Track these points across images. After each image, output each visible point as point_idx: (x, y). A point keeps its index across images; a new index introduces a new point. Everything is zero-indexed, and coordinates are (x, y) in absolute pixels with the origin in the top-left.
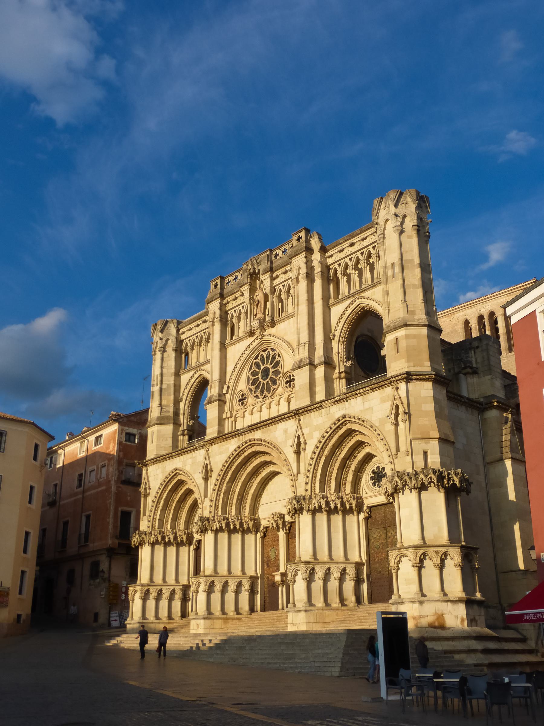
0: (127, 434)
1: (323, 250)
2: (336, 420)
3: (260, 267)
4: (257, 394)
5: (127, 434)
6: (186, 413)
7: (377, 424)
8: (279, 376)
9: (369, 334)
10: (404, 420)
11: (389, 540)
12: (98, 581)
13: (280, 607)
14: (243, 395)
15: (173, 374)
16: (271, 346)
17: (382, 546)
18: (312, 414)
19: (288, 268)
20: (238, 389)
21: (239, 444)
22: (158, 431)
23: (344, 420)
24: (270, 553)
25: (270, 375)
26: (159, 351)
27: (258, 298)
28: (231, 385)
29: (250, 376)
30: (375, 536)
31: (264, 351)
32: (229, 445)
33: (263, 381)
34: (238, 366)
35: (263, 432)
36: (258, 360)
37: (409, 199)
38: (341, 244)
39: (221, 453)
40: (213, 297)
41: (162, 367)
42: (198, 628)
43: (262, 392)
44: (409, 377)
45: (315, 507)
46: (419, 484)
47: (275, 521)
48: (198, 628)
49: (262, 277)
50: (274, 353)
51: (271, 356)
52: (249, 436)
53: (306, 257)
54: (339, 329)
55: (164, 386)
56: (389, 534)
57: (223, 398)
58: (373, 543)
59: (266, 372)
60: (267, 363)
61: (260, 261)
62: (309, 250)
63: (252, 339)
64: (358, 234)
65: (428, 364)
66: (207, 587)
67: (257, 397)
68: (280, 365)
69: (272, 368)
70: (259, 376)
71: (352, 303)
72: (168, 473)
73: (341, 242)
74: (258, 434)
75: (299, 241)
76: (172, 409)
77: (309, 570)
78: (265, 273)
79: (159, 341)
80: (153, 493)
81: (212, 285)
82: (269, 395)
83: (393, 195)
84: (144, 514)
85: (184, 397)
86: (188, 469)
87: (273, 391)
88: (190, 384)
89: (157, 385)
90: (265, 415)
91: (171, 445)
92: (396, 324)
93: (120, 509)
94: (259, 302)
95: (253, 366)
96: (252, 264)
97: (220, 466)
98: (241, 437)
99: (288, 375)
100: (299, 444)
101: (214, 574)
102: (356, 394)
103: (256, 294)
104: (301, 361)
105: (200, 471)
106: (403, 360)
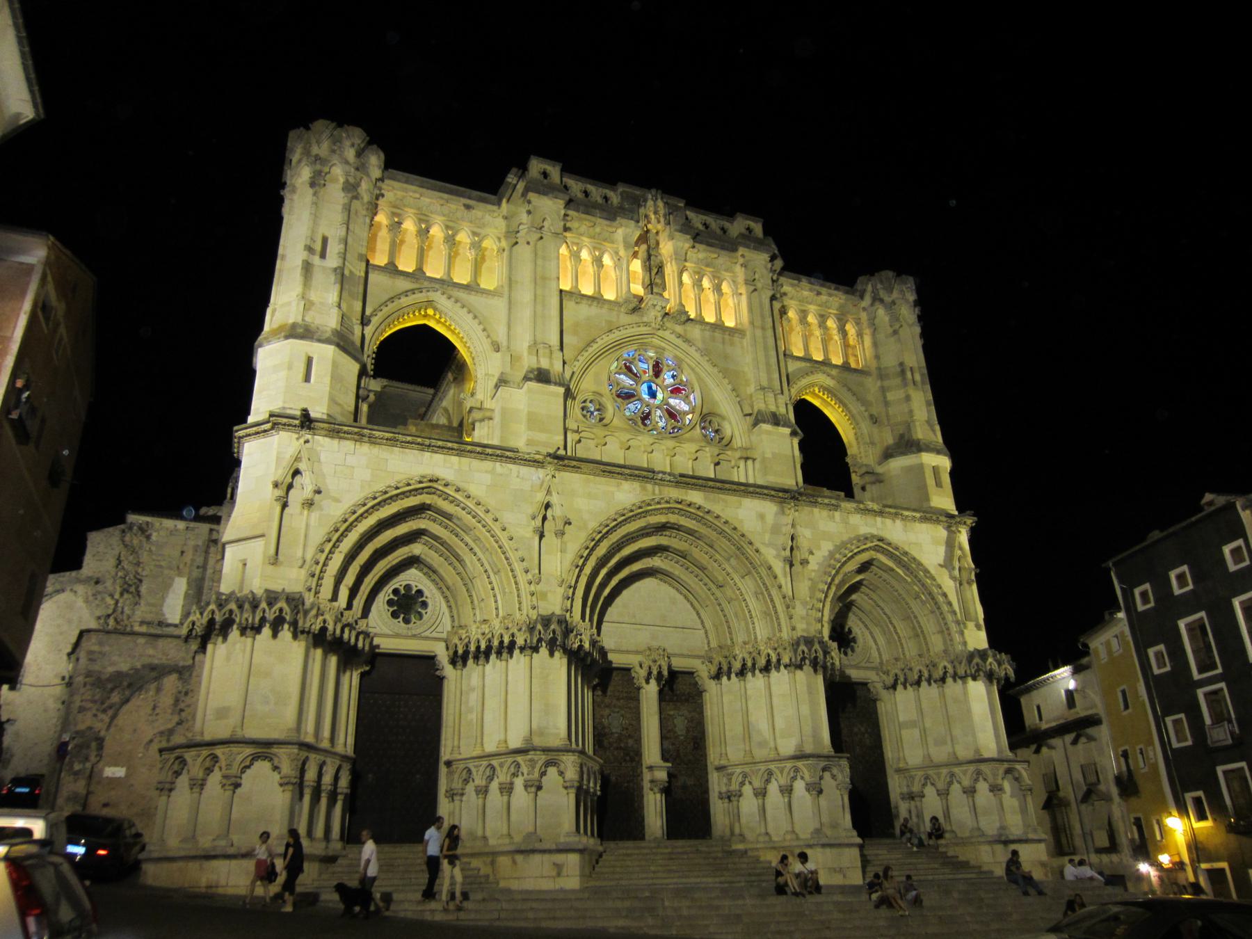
7: (933, 572)
18: (816, 510)
21: (647, 498)
22: (335, 365)
24: (605, 721)
32: (613, 489)
35: (706, 499)
42: (559, 875)
52: (674, 493)
56: (856, 730)
63: (625, 319)
72: (398, 478)
74: (696, 497)
85: (375, 321)
86: (476, 490)
89: (323, 255)
97: (593, 525)
98: (649, 487)
102: (896, 514)
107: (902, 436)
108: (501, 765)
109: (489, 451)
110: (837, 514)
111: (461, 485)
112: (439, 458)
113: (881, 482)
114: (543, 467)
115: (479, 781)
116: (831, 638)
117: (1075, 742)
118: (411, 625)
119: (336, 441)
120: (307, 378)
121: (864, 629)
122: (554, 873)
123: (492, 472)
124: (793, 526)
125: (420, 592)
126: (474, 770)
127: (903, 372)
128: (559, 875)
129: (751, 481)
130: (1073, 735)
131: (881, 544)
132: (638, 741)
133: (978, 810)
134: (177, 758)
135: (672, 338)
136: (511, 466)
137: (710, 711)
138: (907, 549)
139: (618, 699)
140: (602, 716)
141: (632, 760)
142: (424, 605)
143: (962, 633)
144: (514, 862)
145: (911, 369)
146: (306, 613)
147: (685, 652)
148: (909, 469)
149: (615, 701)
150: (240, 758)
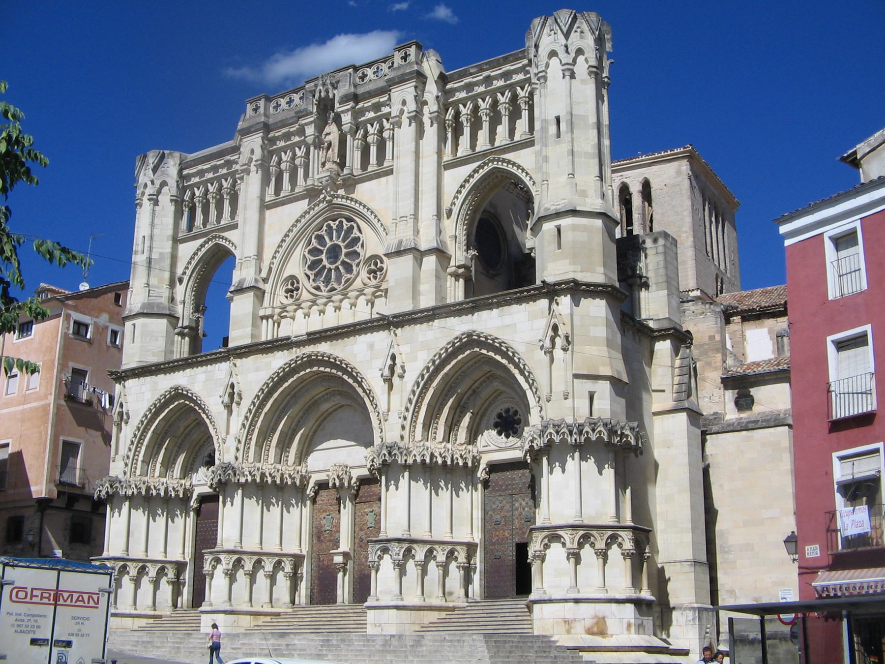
0: (76, 322)
1: (443, 79)
2: (457, 338)
3: (335, 92)
4: (318, 283)
5: (76, 322)
6: (187, 301)
8: (357, 261)
9: (492, 211)
10: (565, 350)
11: (516, 513)
12: (20, 546)
13: (339, 599)
14: (292, 284)
15: (171, 238)
17: (505, 521)
18: (418, 327)
19: (384, 99)
20: (287, 274)
23: (471, 340)
25: (343, 257)
26: (149, 200)
27: (328, 138)
28: (274, 267)
29: (307, 256)
30: (494, 506)
31: (334, 220)
33: (328, 266)
34: (288, 240)
36: (323, 232)
37: (585, 27)
38: (471, 74)
39: (257, 370)
41: (152, 225)
43: (327, 281)
44: (578, 290)
45: (415, 461)
46: (583, 439)
47: (338, 477)
49: (338, 108)
50: (349, 224)
51: (345, 227)
53: (416, 87)
54: (459, 203)
55: (155, 256)
56: (517, 505)
57: (261, 285)
58: (491, 516)
59: (334, 253)
61: (338, 82)
62: (421, 77)
64: (498, 64)
65: (601, 270)
66: (230, 567)
67: (318, 288)
68: (360, 244)
69: (346, 247)
71: (480, 167)
72: (162, 392)
73: (472, 71)
74: (323, 348)
75: (405, 61)
76: (165, 292)
77: (403, 550)
78: (345, 99)
79: (149, 184)
80: (135, 420)
81: (249, 108)
82: (339, 288)
83: (564, 16)
84: (117, 453)
85: (186, 278)
87: (346, 282)
88: (197, 258)
90: (331, 319)
91: (163, 348)
92: (558, 207)
93: (62, 438)
94: (330, 145)
95: (313, 240)
96: (324, 85)
97: (256, 391)
100: (392, 368)
101: (239, 549)
103: (327, 130)
104: (400, 242)
105: (221, 394)
106: (567, 261)
111: (189, 387)
114: (229, 360)
145: (558, 120)
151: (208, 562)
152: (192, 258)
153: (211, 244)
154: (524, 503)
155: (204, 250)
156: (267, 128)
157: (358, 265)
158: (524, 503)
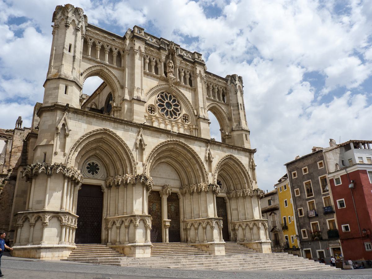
11: (220, 213)
16: (174, 94)
18: (215, 146)
21: (169, 139)
32: (159, 136)
40: (142, 38)
48: (144, 253)
50: (174, 98)
56: (220, 211)
59: (169, 105)
60: (170, 100)
70: (165, 104)
74: (182, 140)
80: (77, 137)
89: (70, 51)
97: (153, 147)
99: (185, 115)
102: (236, 149)
107: (237, 125)
108: (126, 220)
109: (123, 122)
110: (220, 147)
112: (108, 123)
113: (230, 138)
115: (118, 225)
116: (217, 184)
117: (270, 215)
118: (94, 175)
119: (76, 115)
120: (65, 93)
121: (223, 181)
122: (143, 252)
123: (124, 128)
124: (209, 150)
125: (97, 165)
126: (116, 221)
127: (238, 106)
128: (144, 253)
129: (197, 136)
130: (270, 213)
131: (230, 158)
132: (161, 213)
133: (254, 234)
134: (25, 216)
135: (175, 89)
136: (129, 127)
137: (181, 204)
138: (238, 158)
139: (155, 200)
140: (150, 205)
141: (159, 219)
142: (98, 169)
143: (252, 184)
144: (130, 249)
145: (241, 104)
146: (68, 171)
147: (175, 186)
148: (238, 135)
149: (154, 201)
150: (48, 217)
151: (139, 220)
152: (89, 68)
153: (99, 68)
154: (222, 211)
155: (95, 69)
156: (146, 44)
157: (179, 114)
158: (222, 211)
